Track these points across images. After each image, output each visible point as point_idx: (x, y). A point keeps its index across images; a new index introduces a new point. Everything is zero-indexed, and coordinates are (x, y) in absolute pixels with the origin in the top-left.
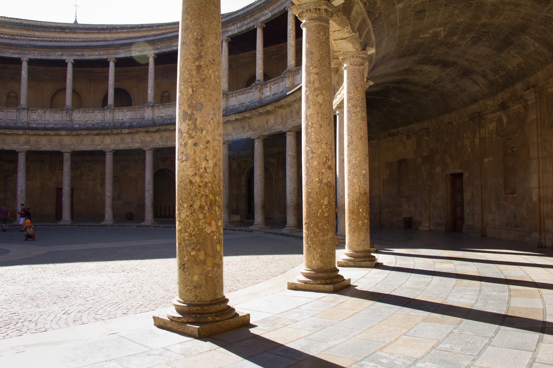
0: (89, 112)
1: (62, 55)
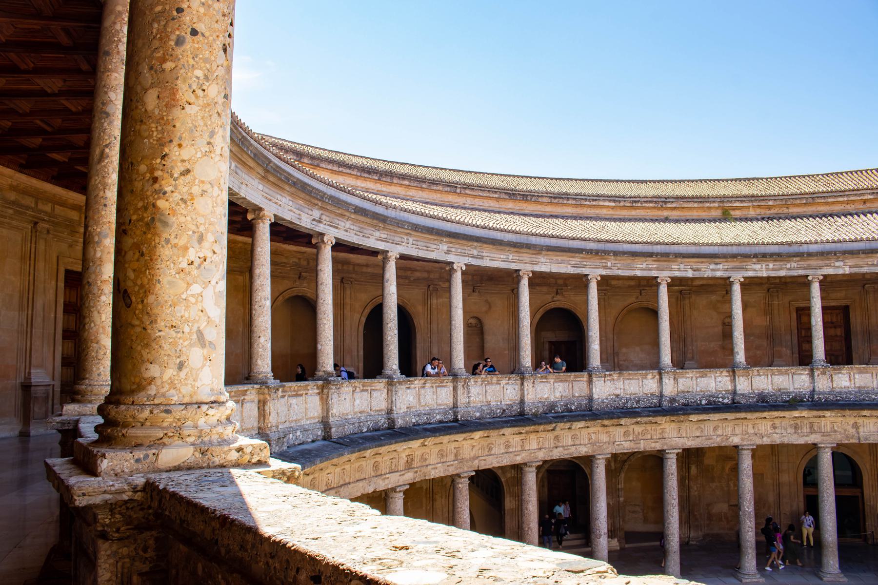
0: (492, 384)
1: (448, 252)
